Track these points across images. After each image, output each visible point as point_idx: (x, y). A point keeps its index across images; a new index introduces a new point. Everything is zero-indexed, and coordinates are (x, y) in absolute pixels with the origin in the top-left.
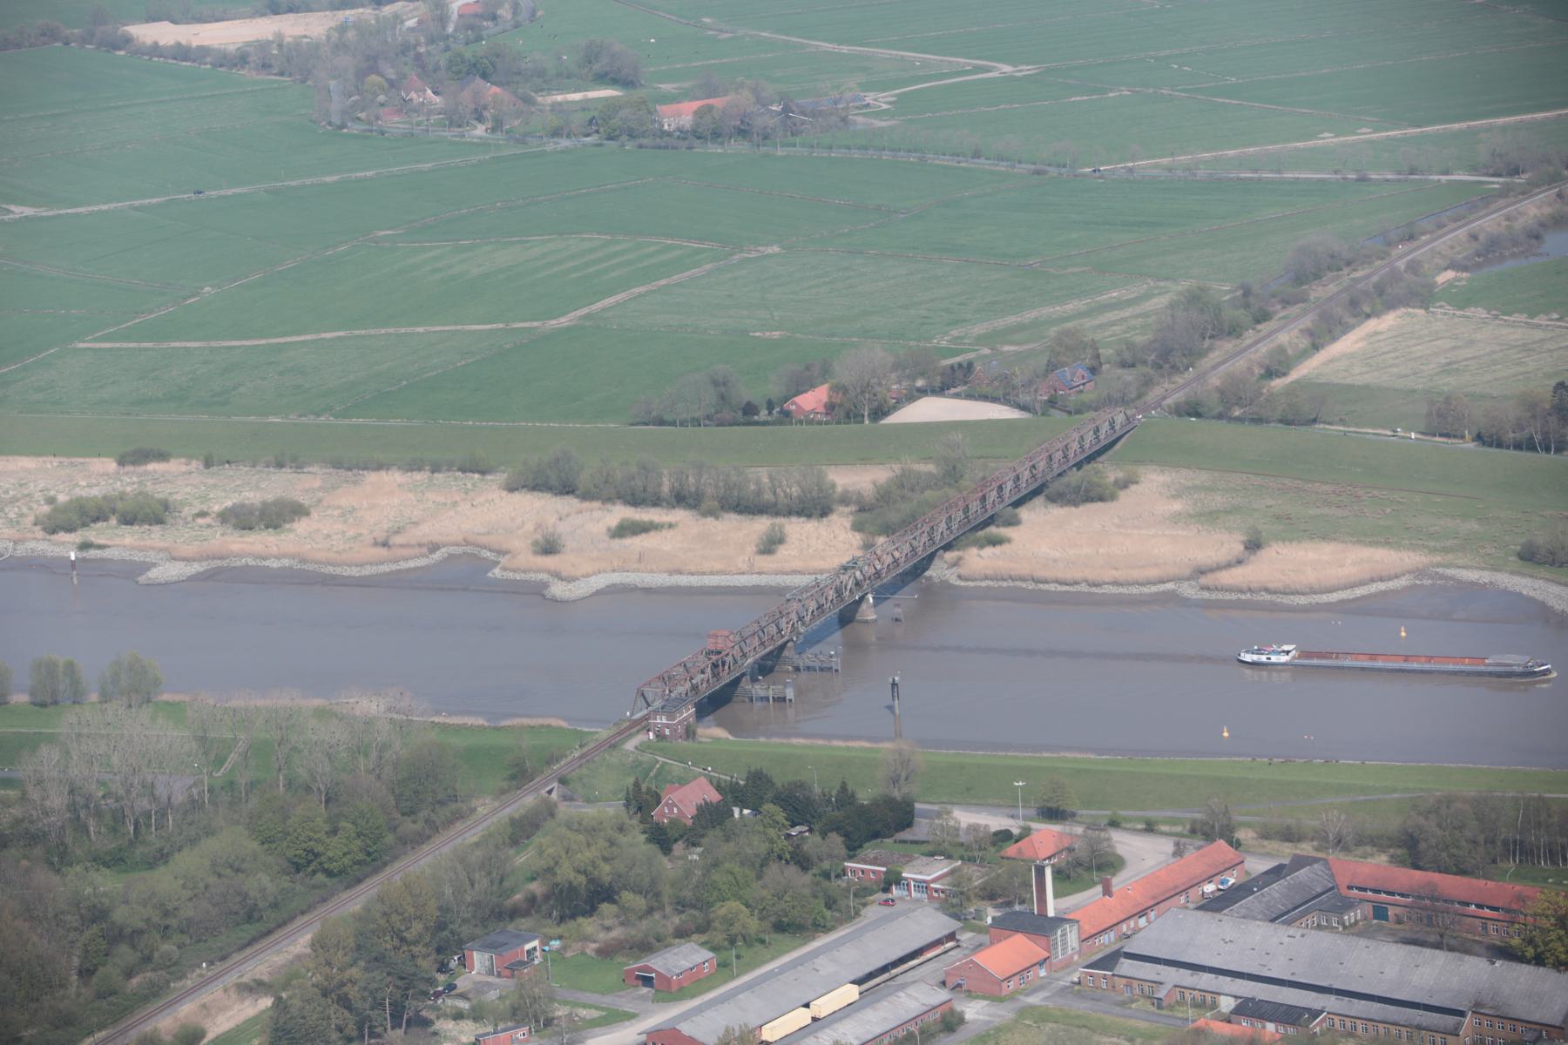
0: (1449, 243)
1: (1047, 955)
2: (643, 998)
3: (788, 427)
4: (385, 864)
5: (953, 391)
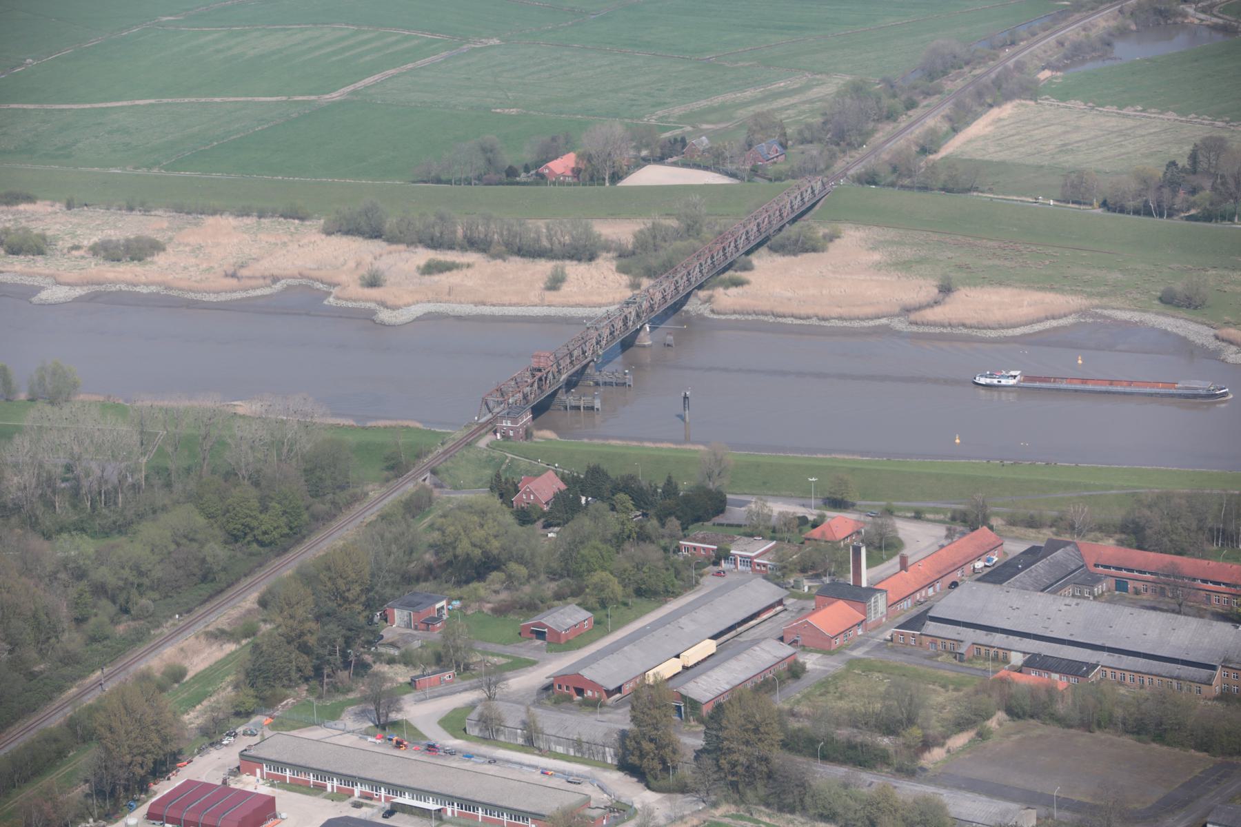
0: (1043, 47)
1: (863, 617)
2: (537, 648)
3: (544, 187)
4: (304, 537)
5: (670, 160)
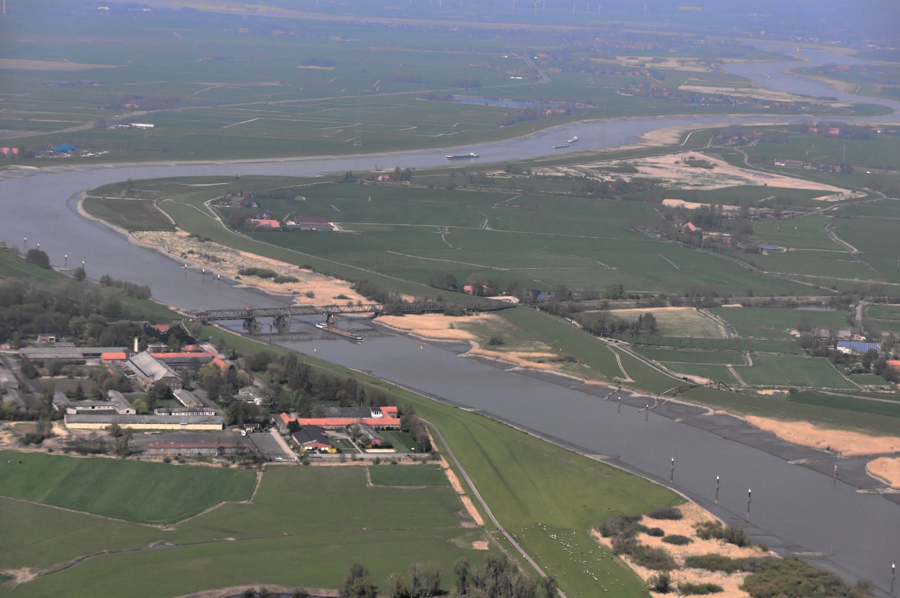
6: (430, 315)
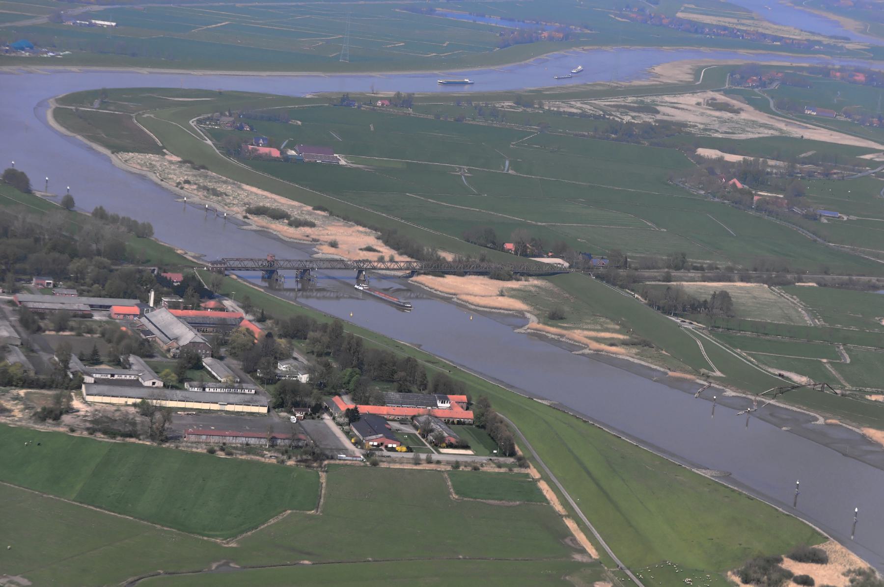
1: (138, 314)
6: (473, 277)
